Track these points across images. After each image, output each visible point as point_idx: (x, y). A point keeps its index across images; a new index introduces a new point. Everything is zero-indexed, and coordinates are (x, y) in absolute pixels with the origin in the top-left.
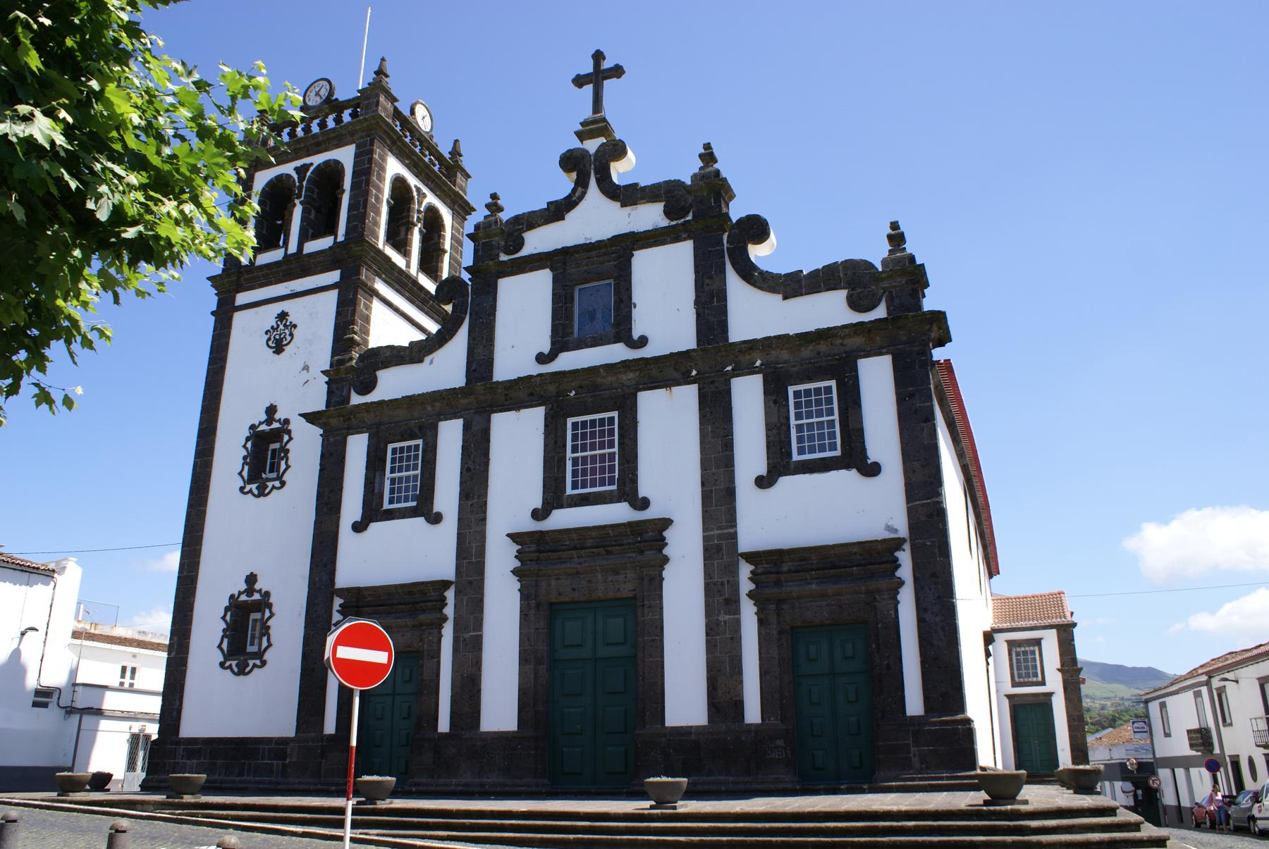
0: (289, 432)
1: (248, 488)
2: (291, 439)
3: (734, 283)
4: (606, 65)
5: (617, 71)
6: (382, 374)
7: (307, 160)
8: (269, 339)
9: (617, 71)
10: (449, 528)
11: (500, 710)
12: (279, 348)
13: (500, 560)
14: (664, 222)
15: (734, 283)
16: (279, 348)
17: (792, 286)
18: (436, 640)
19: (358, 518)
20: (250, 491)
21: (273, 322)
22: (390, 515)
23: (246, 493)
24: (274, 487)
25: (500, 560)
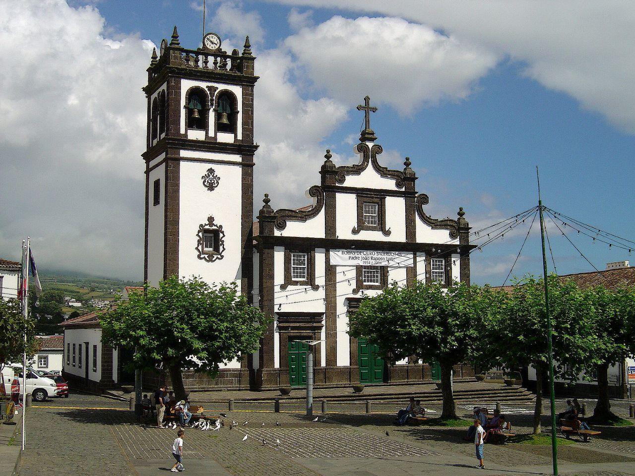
0: (223, 232)
1: (202, 256)
2: (224, 236)
3: (418, 222)
4: (371, 113)
5: (367, 99)
6: (289, 224)
7: (215, 85)
8: (204, 182)
9: (367, 99)
10: (321, 293)
11: (343, 359)
12: (211, 187)
13: (341, 308)
14: (395, 189)
15: (418, 222)
16: (211, 187)
17: (435, 224)
18: (122, 365)
19: (283, 282)
20: (204, 258)
21: (205, 173)
22: (296, 283)
23: (201, 259)
24: (217, 258)
25: (341, 308)
